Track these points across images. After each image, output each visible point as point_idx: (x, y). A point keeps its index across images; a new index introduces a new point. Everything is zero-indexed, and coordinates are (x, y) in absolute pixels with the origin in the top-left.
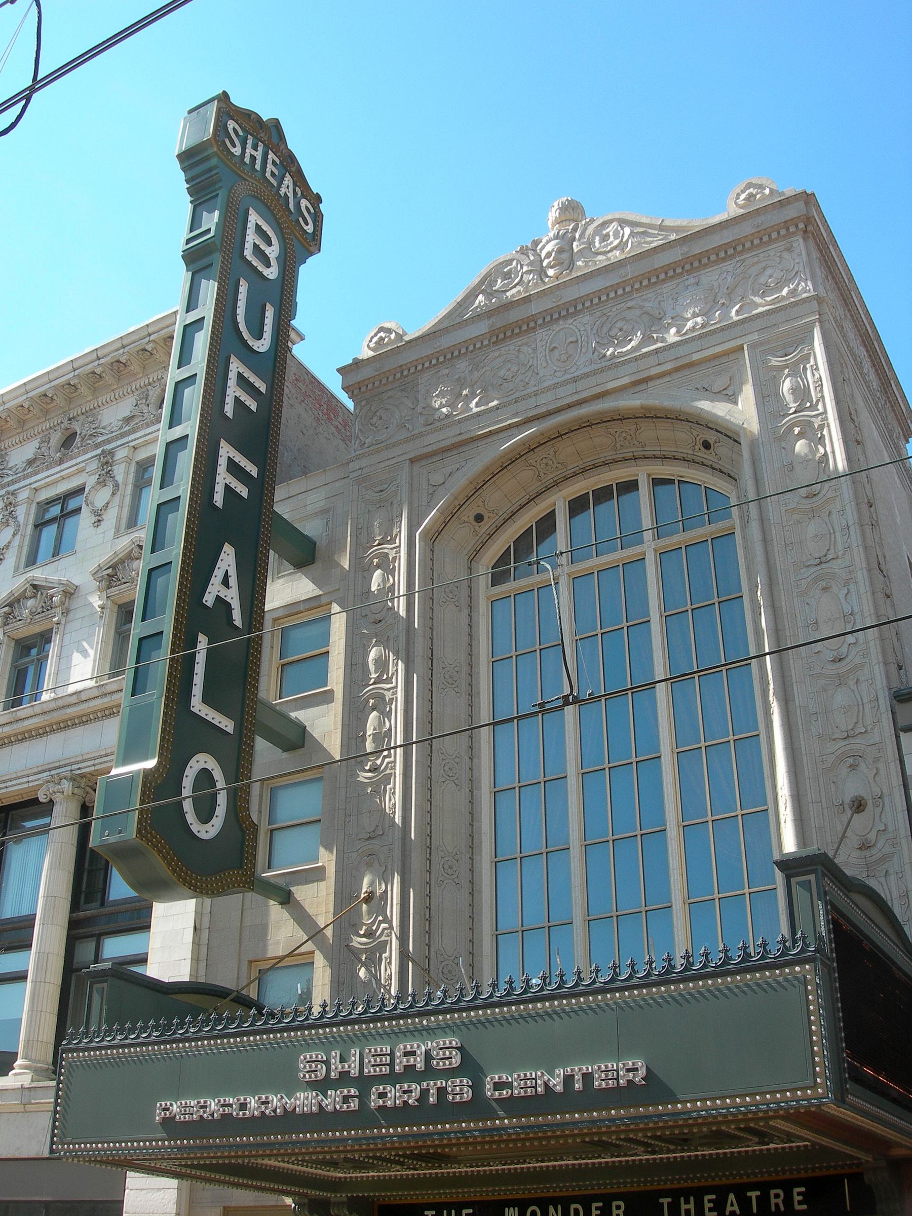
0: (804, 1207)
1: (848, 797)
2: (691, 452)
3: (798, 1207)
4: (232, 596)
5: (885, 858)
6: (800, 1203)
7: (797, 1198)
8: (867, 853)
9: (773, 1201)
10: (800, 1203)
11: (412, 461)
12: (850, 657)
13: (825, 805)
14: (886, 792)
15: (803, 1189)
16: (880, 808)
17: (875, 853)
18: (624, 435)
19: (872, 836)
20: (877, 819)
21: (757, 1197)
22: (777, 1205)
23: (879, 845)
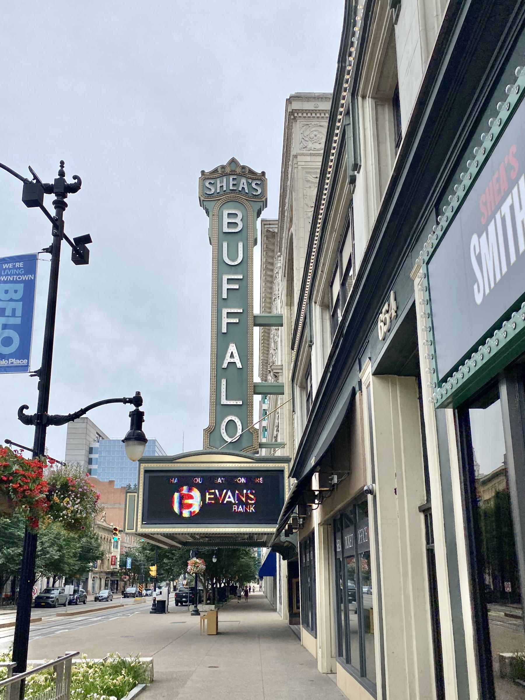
4: (237, 360)
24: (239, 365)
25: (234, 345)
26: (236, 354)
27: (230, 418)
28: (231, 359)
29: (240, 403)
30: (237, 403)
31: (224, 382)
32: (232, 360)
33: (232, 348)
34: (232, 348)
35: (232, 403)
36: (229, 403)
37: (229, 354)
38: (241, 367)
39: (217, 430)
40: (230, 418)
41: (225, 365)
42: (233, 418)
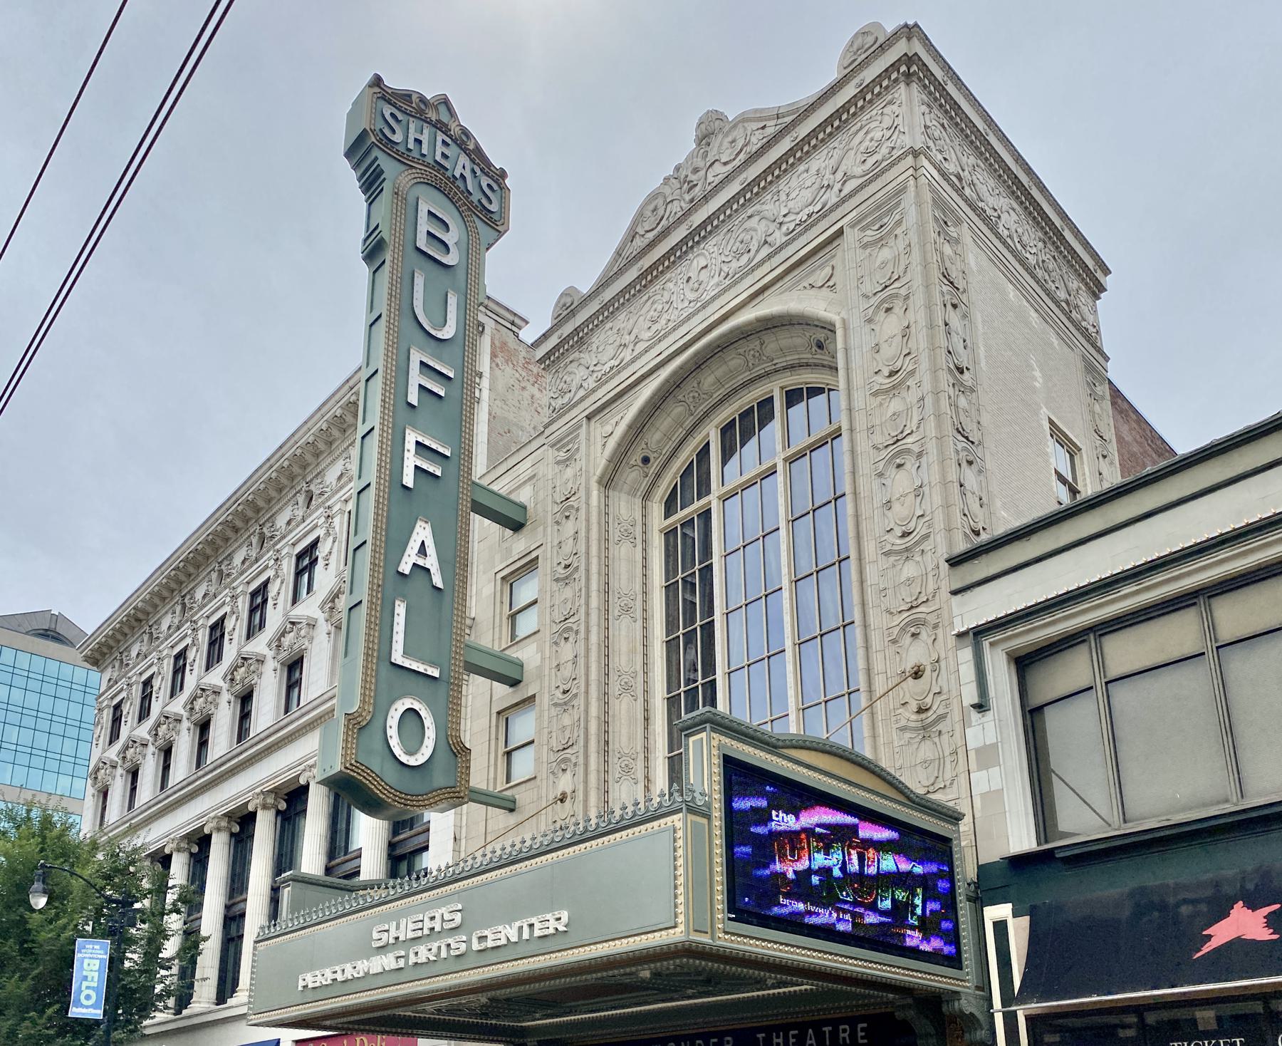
0: (866, 1041)
1: (909, 666)
2: (810, 356)
3: (861, 1041)
5: (942, 718)
6: (862, 1038)
7: (860, 1034)
8: (923, 716)
9: (842, 1035)
10: (862, 1038)
11: (589, 418)
12: (917, 530)
13: (889, 676)
14: (943, 656)
15: (865, 1025)
16: (937, 672)
17: (931, 716)
18: (752, 352)
19: (929, 700)
20: (934, 682)
21: (829, 1031)
22: (844, 1038)
23: (934, 708)
24: (438, 580)
25: (428, 527)
26: (431, 550)
27: (408, 703)
28: (417, 558)
29: (436, 673)
30: (426, 670)
31: (400, 609)
32: (421, 562)
33: (423, 533)
34: (423, 533)
35: (415, 666)
36: (407, 663)
37: (414, 546)
38: (440, 585)
39: (377, 724)
40: (408, 703)
41: (406, 568)
42: (416, 706)
